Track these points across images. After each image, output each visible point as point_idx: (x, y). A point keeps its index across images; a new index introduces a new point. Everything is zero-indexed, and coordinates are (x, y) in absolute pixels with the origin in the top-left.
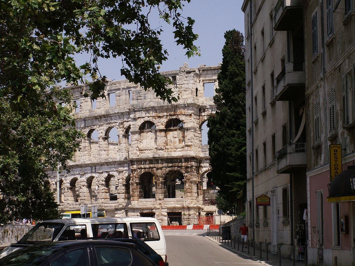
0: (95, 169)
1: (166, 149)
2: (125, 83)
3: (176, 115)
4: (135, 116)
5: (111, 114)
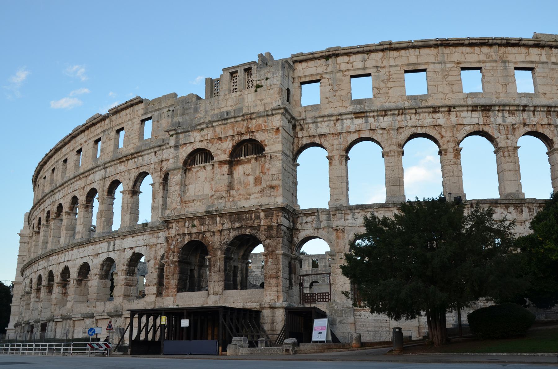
0: (114, 245)
3: (250, 132)
4: (177, 141)
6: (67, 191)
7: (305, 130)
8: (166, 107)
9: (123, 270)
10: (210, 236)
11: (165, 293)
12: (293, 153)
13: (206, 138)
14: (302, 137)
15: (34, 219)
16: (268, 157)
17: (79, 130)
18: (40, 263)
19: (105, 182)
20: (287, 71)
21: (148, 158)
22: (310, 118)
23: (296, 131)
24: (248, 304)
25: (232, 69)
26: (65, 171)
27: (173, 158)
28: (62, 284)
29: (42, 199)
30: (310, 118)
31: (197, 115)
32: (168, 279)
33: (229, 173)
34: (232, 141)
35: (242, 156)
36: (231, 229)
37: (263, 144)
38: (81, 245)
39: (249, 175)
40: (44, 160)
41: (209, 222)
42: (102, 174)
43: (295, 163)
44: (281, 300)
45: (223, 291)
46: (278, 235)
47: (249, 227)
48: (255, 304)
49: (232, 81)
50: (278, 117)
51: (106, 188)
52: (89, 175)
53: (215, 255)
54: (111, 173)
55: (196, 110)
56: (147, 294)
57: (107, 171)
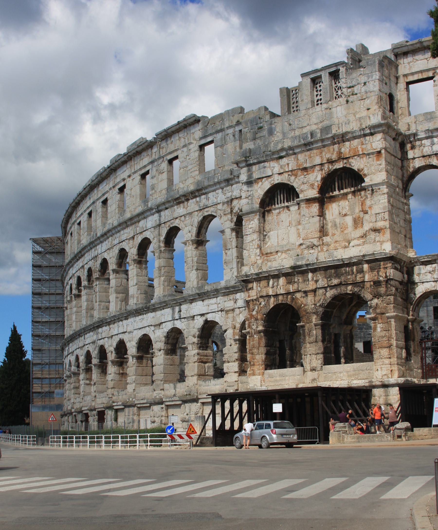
0: (180, 311)
1: (323, 244)
2: (233, 116)
4: (250, 176)
5: (206, 188)
6: (112, 242)
7: (417, 148)
8: (230, 127)
9: (194, 343)
10: (301, 297)
11: (250, 371)
12: (402, 180)
13: (287, 170)
14: (414, 158)
15: (71, 278)
16: (369, 190)
17: (119, 162)
18: (86, 336)
19: (161, 230)
20: (387, 69)
21: (213, 196)
22: (422, 131)
23: (405, 150)
24: (355, 382)
25: (313, 73)
26: (105, 216)
27: (246, 198)
28: (117, 362)
29: (80, 252)
30: (422, 131)
31: (273, 139)
32: (252, 354)
33: (320, 215)
34: (320, 172)
35: (335, 191)
36: (327, 287)
37: (361, 173)
38: (138, 312)
40: (76, 201)
41: (298, 280)
42: (155, 219)
43: (407, 194)
44: (396, 374)
45: (322, 367)
46: (388, 293)
47: (350, 284)
48: (363, 381)
49: (315, 90)
50: (379, 136)
51: (162, 238)
52: (139, 222)
53: (310, 321)
54: (167, 217)
55: (271, 132)
56: (227, 373)
57: (162, 214)
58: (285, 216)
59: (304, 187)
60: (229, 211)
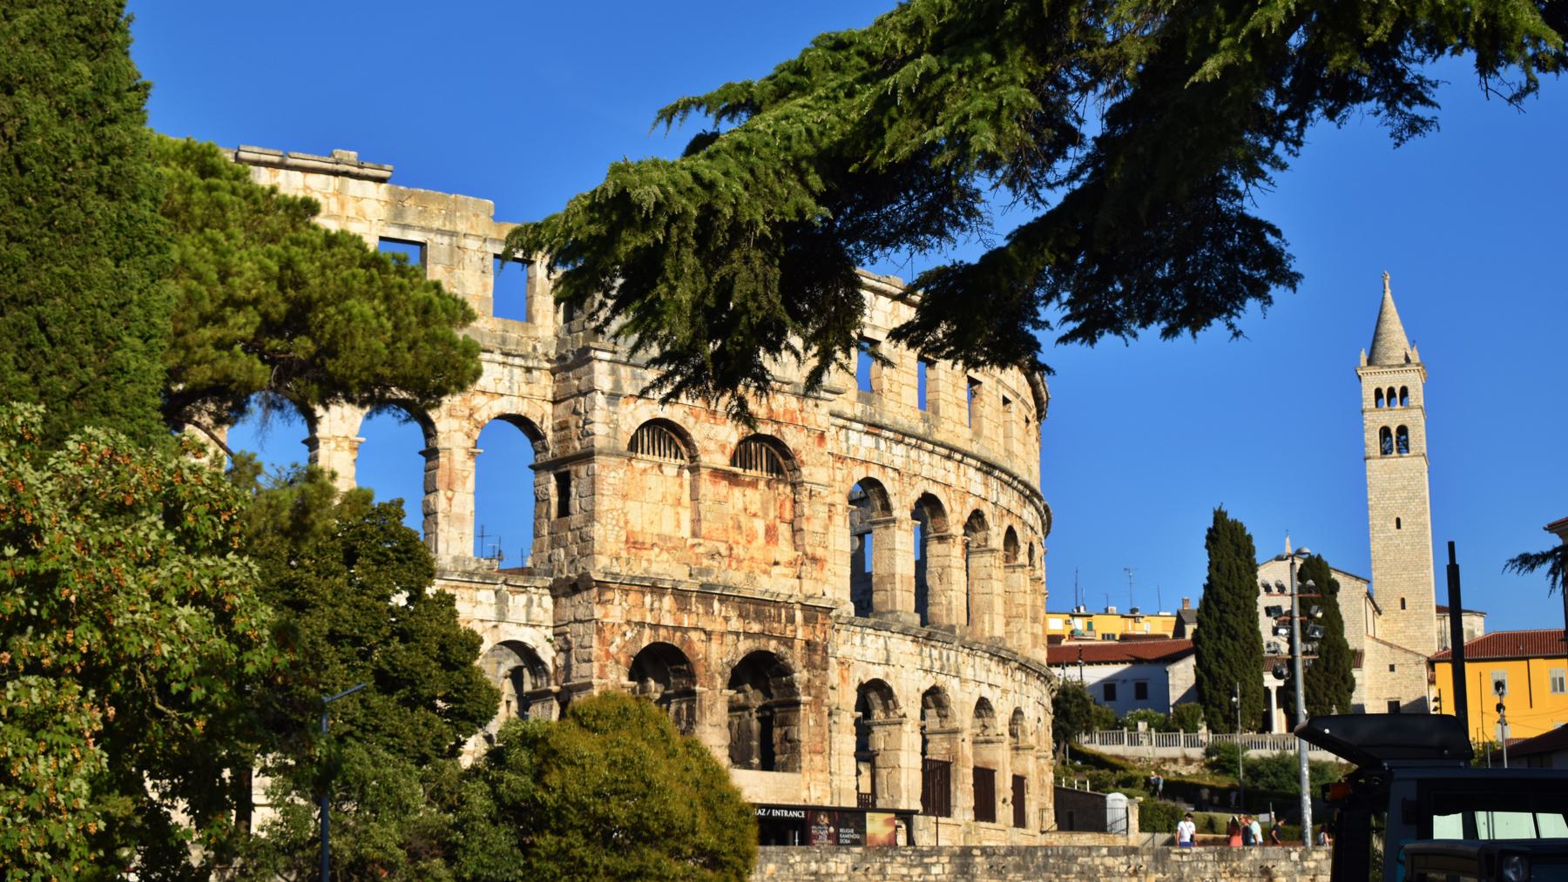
4: (617, 383)
39: (755, 515)
47: (775, 638)
58: (653, 479)
59: (712, 446)
60: (467, 413)
